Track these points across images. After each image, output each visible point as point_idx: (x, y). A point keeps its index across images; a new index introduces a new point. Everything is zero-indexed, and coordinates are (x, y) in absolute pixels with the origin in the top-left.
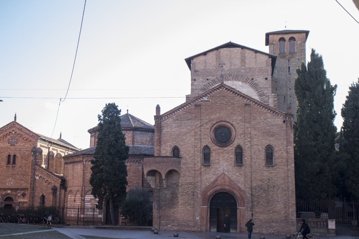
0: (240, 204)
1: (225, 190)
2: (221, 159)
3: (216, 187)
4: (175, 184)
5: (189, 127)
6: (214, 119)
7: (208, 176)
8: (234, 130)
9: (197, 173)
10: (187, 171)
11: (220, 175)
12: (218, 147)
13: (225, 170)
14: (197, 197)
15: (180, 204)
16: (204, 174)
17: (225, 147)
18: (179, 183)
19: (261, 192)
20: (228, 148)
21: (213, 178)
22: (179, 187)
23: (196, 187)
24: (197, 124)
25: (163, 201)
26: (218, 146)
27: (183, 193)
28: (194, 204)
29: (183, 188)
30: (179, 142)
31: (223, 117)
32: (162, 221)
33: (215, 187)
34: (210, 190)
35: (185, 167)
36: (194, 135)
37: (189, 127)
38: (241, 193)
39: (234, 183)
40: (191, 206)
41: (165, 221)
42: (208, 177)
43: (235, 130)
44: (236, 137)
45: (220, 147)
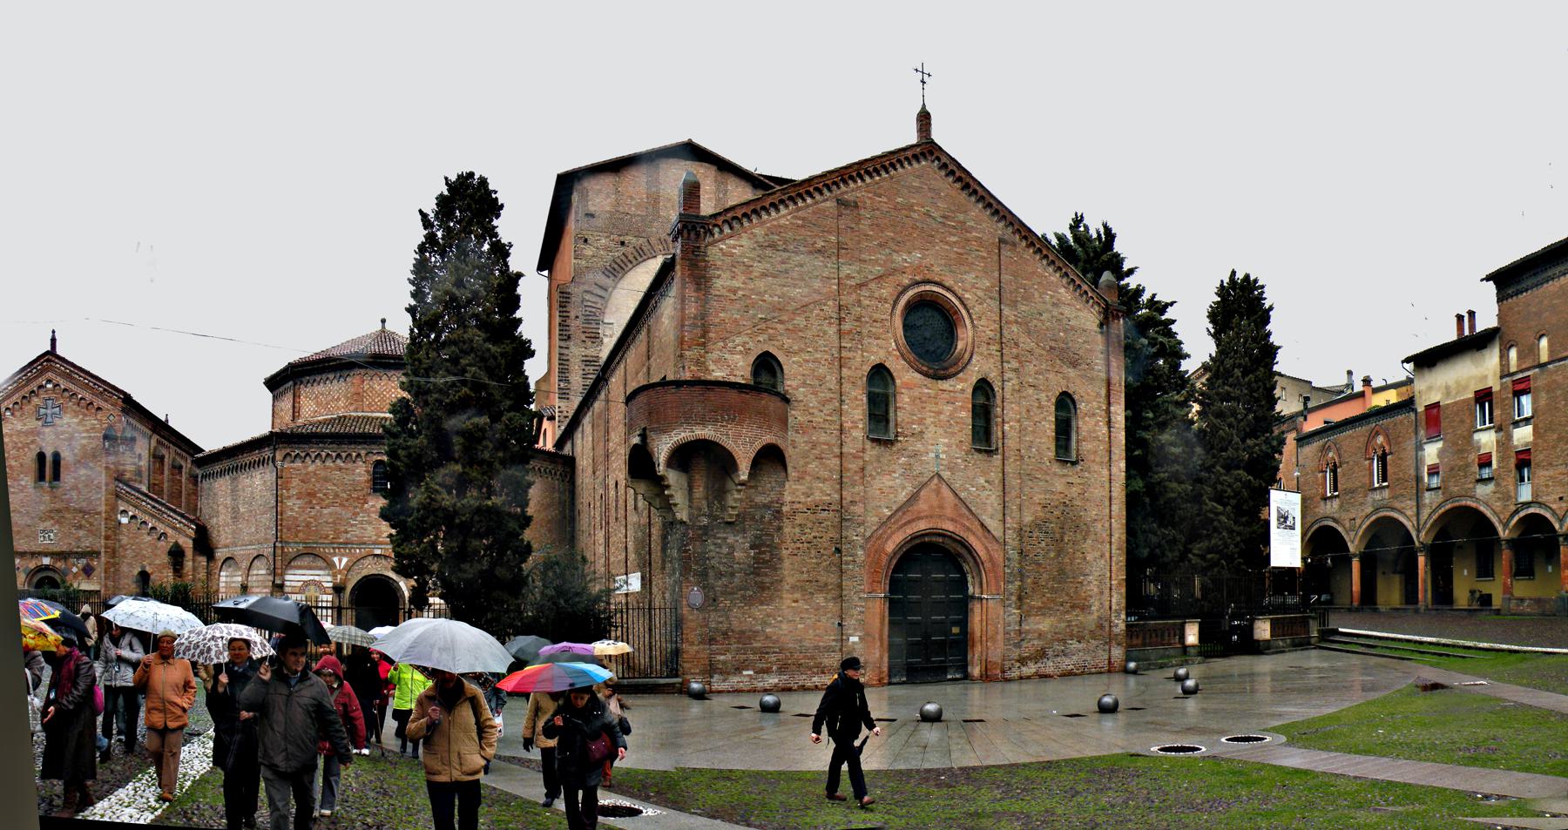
0: (985, 586)
1: (940, 535)
2: (928, 421)
3: (914, 524)
4: (767, 506)
5: (817, 284)
6: (906, 267)
7: (887, 481)
8: (968, 321)
9: (850, 466)
10: (812, 456)
11: (926, 479)
12: (919, 376)
13: (944, 463)
14: (851, 558)
15: (787, 587)
16: (874, 473)
17: (942, 379)
18: (782, 504)
19: (1043, 544)
20: (952, 383)
21: (904, 488)
22: (785, 520)
23: (846, 520)
24: (849, 277)
25: (720, 575)
26: (920, 373)
27: (798, 545)
28: (840, 586)
29: (798, 522)
30: (779, 338)
31: (932, 265)
32: (722, 654)
33: (909, 522)
34: (893, 533)
35: (804, 442)
36: (835, 315)
37: (817, 284)
38: (989, 545)
39: (970, 511)
40: (829, 596)
41: (729, 656)
42: (890, 483)
43: (972, 322)
44: (976, 349)
45: (926, 375)
